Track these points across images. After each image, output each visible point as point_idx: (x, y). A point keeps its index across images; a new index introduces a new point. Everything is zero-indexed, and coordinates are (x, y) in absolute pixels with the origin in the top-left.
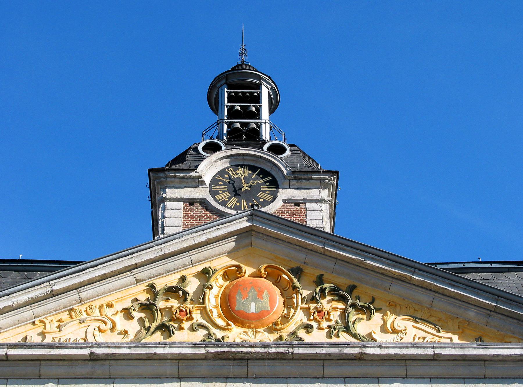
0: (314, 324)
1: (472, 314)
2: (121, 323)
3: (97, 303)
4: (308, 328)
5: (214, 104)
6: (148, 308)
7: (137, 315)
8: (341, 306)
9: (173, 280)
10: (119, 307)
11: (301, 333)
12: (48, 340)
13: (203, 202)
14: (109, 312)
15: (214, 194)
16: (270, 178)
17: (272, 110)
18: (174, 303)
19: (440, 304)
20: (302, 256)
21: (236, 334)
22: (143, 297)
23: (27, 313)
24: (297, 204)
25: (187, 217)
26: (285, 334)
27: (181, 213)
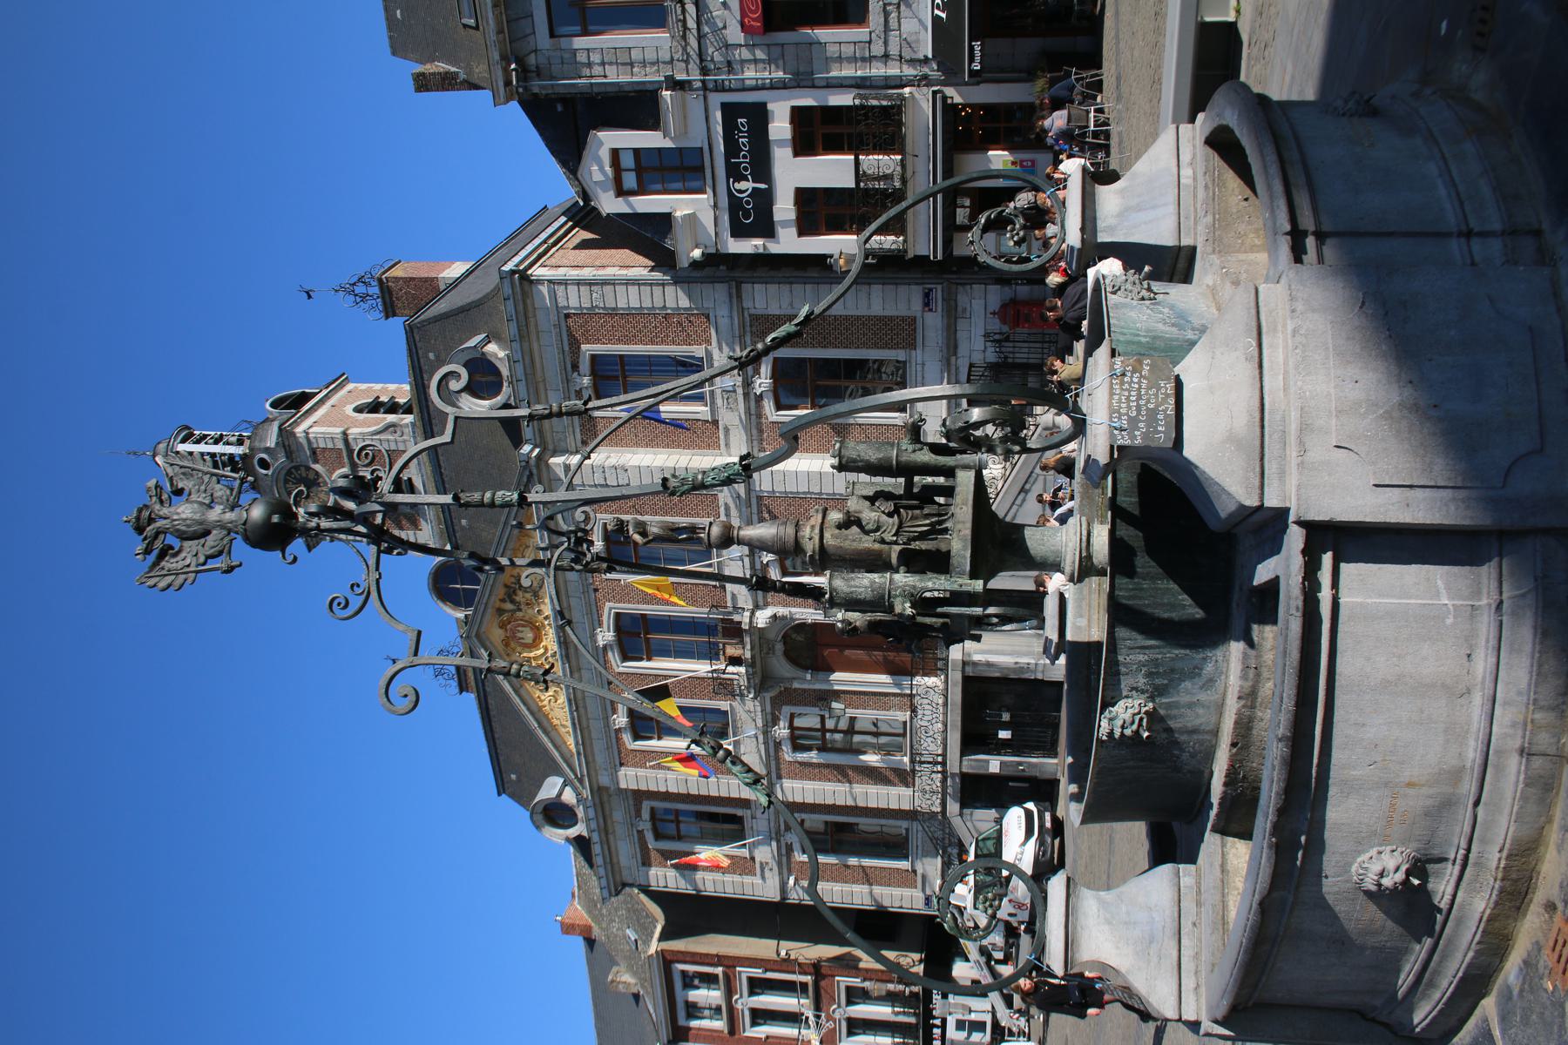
8: (520, 593)
10: (538, 693)
12: (569, 723)
19: (511, 545)
20: (490, 611)
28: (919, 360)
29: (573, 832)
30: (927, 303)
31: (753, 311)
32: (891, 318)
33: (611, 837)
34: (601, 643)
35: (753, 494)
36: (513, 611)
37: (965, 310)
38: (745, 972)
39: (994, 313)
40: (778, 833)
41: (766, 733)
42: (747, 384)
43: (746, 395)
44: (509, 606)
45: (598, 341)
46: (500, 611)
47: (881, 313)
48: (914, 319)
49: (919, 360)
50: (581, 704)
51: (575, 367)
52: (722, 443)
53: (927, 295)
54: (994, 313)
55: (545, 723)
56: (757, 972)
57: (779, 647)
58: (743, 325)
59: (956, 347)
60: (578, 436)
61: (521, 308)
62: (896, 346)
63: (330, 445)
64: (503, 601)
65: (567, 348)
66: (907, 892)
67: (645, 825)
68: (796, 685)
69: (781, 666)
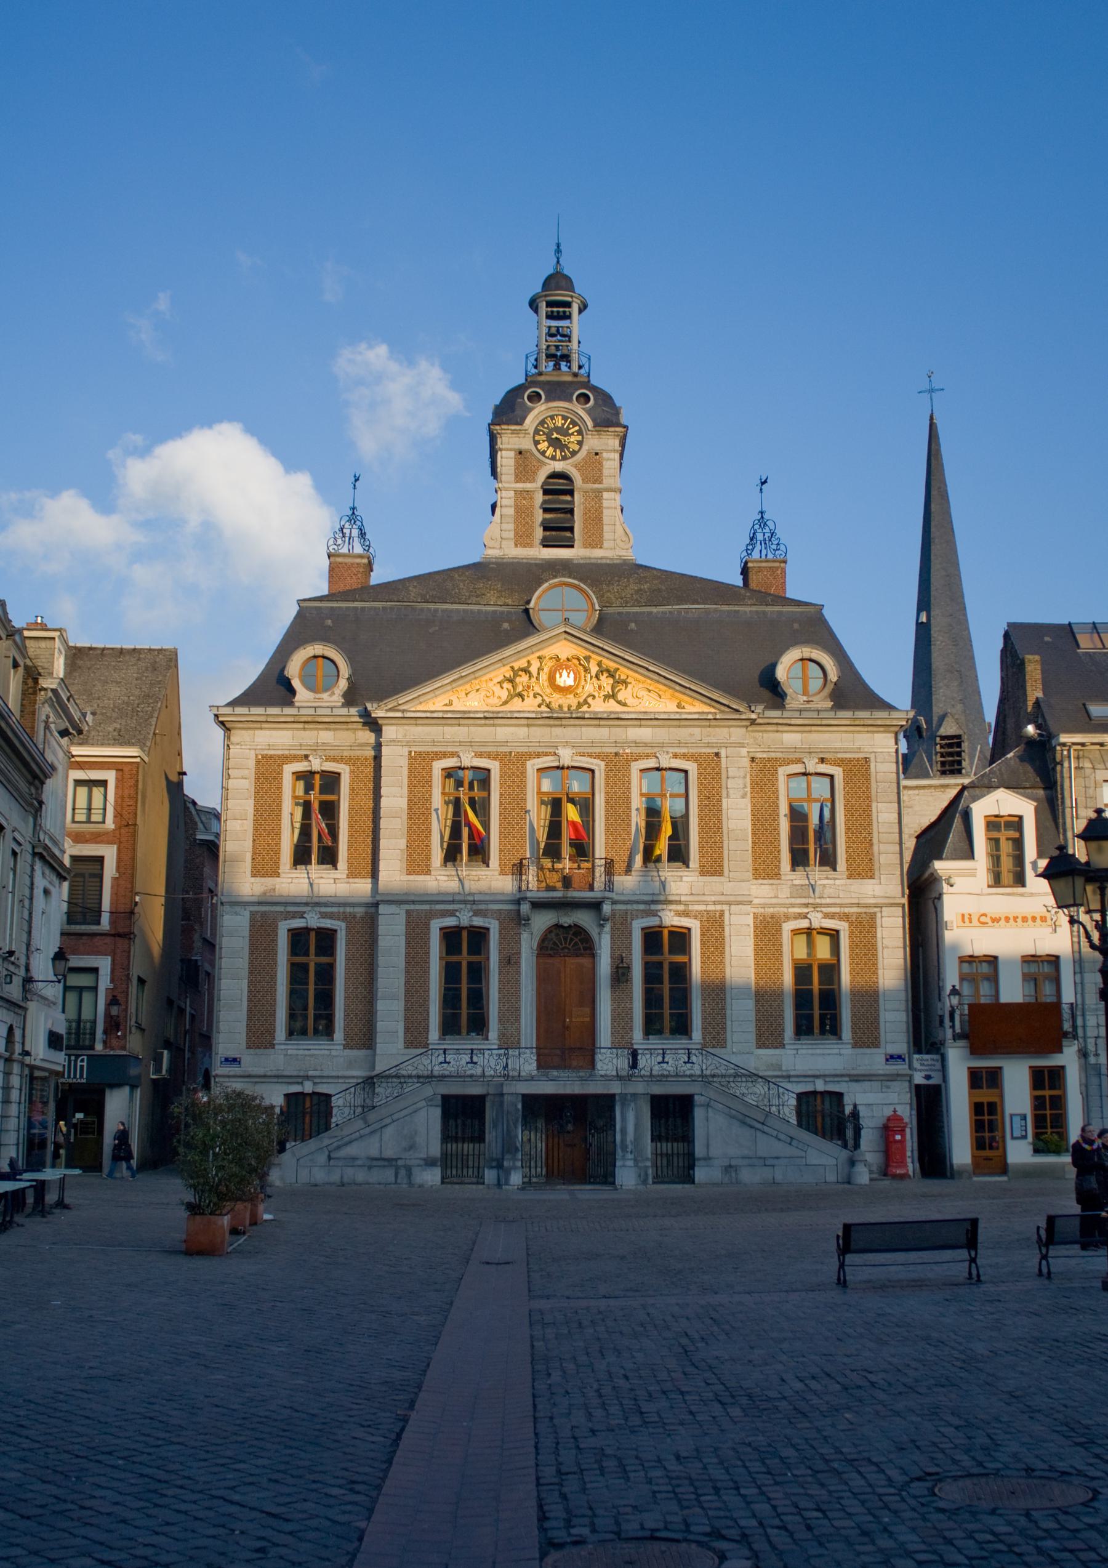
0: (596, 694)
1: (678, 687)
2: (497, 689)
3: (484, 679)
4: (594, 697)
5: (536, 311)
6: (511, 681)
7: (506, 685)
8: (611, 681)
9: (522, 663)
11: (590, 700)
13: (528, 451)
14: (491, 684)
15: (536, 443)
16: (577, 428)
17: (580, 311)
18: (523, 679)
21: (557, 700)
22: (509, 674)
23: (449, 687)
24: (597, 454)
25: (517, 466)
26: (581, 701)
27: (512, 462)
28: (842, 1051)
29: (296, 683)
30: (891, 1058)
31: (879, 915)
32: (877, 1028)
33: (301, 726)
34: (561, 751)
35: (725, 907)
36: (587, 670)
37: (888, 1087)
38: (110, 853)
39: (895, 1111)
40: (318, 904)
41: (465, 902)
42: (815, 906)
43: (806, 905)
44: (594, 669)
45: (846, 783)
46: (587, 659)
47: (882, 1020)
48: (877, 1046)
49: (842, 1051)
50: (491, 722)
51: (822, 760)
52: (760, 881)
53: (899, 1057)
54: (895, 1111)
55: (461, 682)
56: (110, 870)
57: (567, 920)
58: (867, 906)
59: (857, 1081)
60: (759, 755)
61: (879, 722)
62: (854, 1032)
63: (605, 472)
64: (599, 664)
65: (840, 756)
66: (242, 1037)
67: (316, 764)
68: (525, 936)
69: (542, 921)
